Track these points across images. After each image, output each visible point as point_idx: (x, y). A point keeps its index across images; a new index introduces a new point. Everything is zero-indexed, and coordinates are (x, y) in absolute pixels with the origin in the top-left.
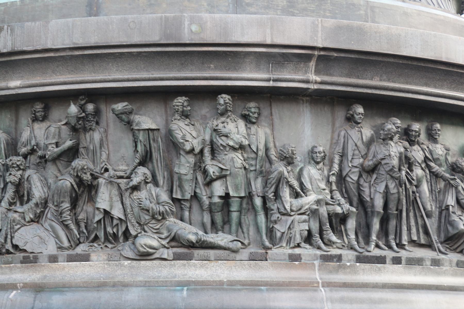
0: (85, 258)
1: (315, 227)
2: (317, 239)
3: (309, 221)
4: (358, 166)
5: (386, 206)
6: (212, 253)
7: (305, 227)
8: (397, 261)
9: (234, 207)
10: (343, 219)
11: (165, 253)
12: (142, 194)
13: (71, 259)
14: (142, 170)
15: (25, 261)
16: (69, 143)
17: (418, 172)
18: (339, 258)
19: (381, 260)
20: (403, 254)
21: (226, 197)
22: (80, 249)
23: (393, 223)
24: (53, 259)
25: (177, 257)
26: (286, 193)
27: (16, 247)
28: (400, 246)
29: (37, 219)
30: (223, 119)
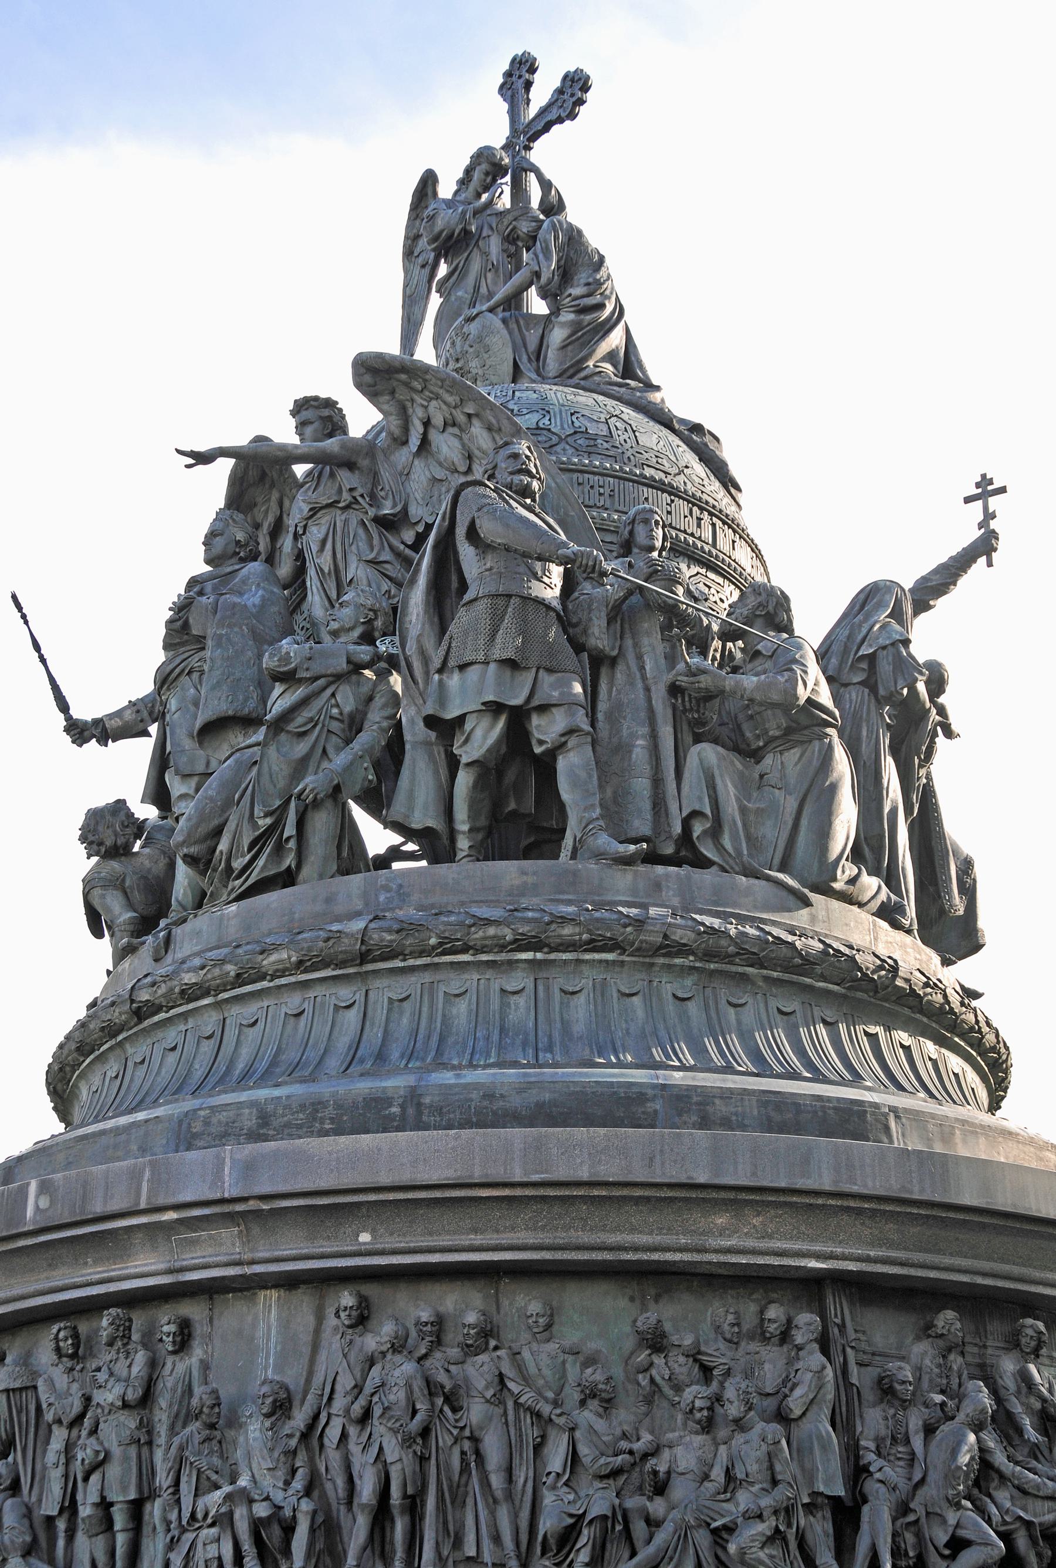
3: (218, 1540)
4: (341, 1413)
7: (212, 1551)
9: (120, 1520)
10: (289, 1529)
17: (476, 1412)
21: (105, 1505)
30: (113, 1355)
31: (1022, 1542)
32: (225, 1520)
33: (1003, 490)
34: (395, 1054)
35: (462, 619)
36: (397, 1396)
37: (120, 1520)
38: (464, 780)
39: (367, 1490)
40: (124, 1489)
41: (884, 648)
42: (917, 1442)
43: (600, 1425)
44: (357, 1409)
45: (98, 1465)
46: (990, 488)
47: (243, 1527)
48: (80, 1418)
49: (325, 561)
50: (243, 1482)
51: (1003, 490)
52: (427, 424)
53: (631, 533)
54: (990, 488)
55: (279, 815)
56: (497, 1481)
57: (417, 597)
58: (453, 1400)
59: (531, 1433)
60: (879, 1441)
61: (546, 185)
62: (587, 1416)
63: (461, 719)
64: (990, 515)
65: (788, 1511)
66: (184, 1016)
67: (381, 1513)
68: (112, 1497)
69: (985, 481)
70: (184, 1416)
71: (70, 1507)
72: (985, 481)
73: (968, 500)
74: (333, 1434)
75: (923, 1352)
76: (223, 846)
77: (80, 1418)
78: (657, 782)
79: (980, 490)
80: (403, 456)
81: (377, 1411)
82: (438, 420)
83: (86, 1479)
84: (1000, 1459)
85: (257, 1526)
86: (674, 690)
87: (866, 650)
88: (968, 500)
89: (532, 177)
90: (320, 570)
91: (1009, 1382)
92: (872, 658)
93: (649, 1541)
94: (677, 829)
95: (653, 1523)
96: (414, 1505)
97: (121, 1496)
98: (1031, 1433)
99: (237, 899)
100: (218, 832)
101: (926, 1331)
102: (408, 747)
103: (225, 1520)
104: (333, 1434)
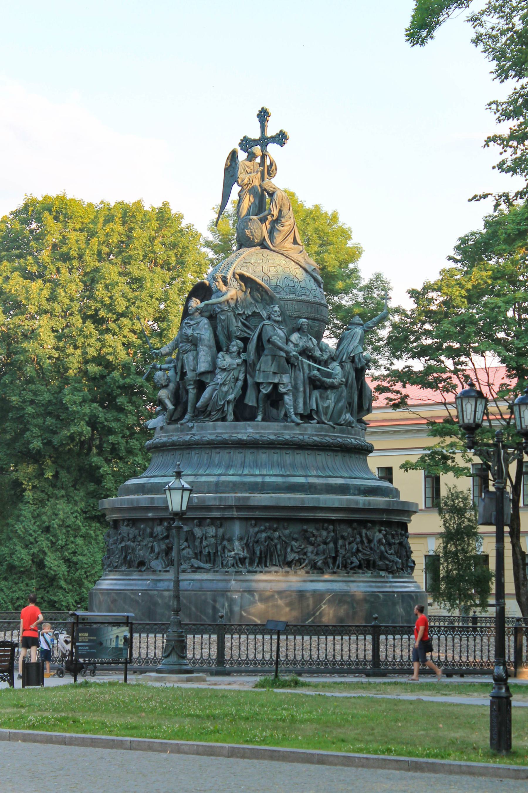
0: (168, 571)
2: (235, 565)
5: (261, 554)
8: (261, 572)
11: (189, 570)
12: (184, 552)
14: (186, 543)
15: (153, 571)
16: (165, 534)
18: (241, 572)
19: (255, 572)
20: (267, 569)
21: (209, 552)
22: (168, 569)
23: (264, 559)
24: (160, 571)
25: (193, 572)
26: (226, 551)
28: (266, 566)
29: (157, 558)
31: (362, 562)
32: (234, 558)
35: (263, 358)
38: (261, 394)
39: (258, 553)
43: (296, 544)
48: (202, 538)
50: (236, 551)
55: (224, 405)
56: (279, 553)
58: (272, 540)
59: (285, 545)
60: (341, 546)
62: (293, 543)
65: (326, 558)
67: (260, 558)
71: (201, 552)
74: (251, 545)
75: (350, 530)
76: (209, 409)
77: (202, 538)
78: (305, 398)
83: (205, 548)
84: (360, 549)
86: (310, 378)
87: (352, 355)
90: (222, 326)
91: (364, 535)
95: (304, 560)
96: (266, 557)
98: (366, 544)
100: (207, 406)
101: (351, 526)
104: (251, 545)
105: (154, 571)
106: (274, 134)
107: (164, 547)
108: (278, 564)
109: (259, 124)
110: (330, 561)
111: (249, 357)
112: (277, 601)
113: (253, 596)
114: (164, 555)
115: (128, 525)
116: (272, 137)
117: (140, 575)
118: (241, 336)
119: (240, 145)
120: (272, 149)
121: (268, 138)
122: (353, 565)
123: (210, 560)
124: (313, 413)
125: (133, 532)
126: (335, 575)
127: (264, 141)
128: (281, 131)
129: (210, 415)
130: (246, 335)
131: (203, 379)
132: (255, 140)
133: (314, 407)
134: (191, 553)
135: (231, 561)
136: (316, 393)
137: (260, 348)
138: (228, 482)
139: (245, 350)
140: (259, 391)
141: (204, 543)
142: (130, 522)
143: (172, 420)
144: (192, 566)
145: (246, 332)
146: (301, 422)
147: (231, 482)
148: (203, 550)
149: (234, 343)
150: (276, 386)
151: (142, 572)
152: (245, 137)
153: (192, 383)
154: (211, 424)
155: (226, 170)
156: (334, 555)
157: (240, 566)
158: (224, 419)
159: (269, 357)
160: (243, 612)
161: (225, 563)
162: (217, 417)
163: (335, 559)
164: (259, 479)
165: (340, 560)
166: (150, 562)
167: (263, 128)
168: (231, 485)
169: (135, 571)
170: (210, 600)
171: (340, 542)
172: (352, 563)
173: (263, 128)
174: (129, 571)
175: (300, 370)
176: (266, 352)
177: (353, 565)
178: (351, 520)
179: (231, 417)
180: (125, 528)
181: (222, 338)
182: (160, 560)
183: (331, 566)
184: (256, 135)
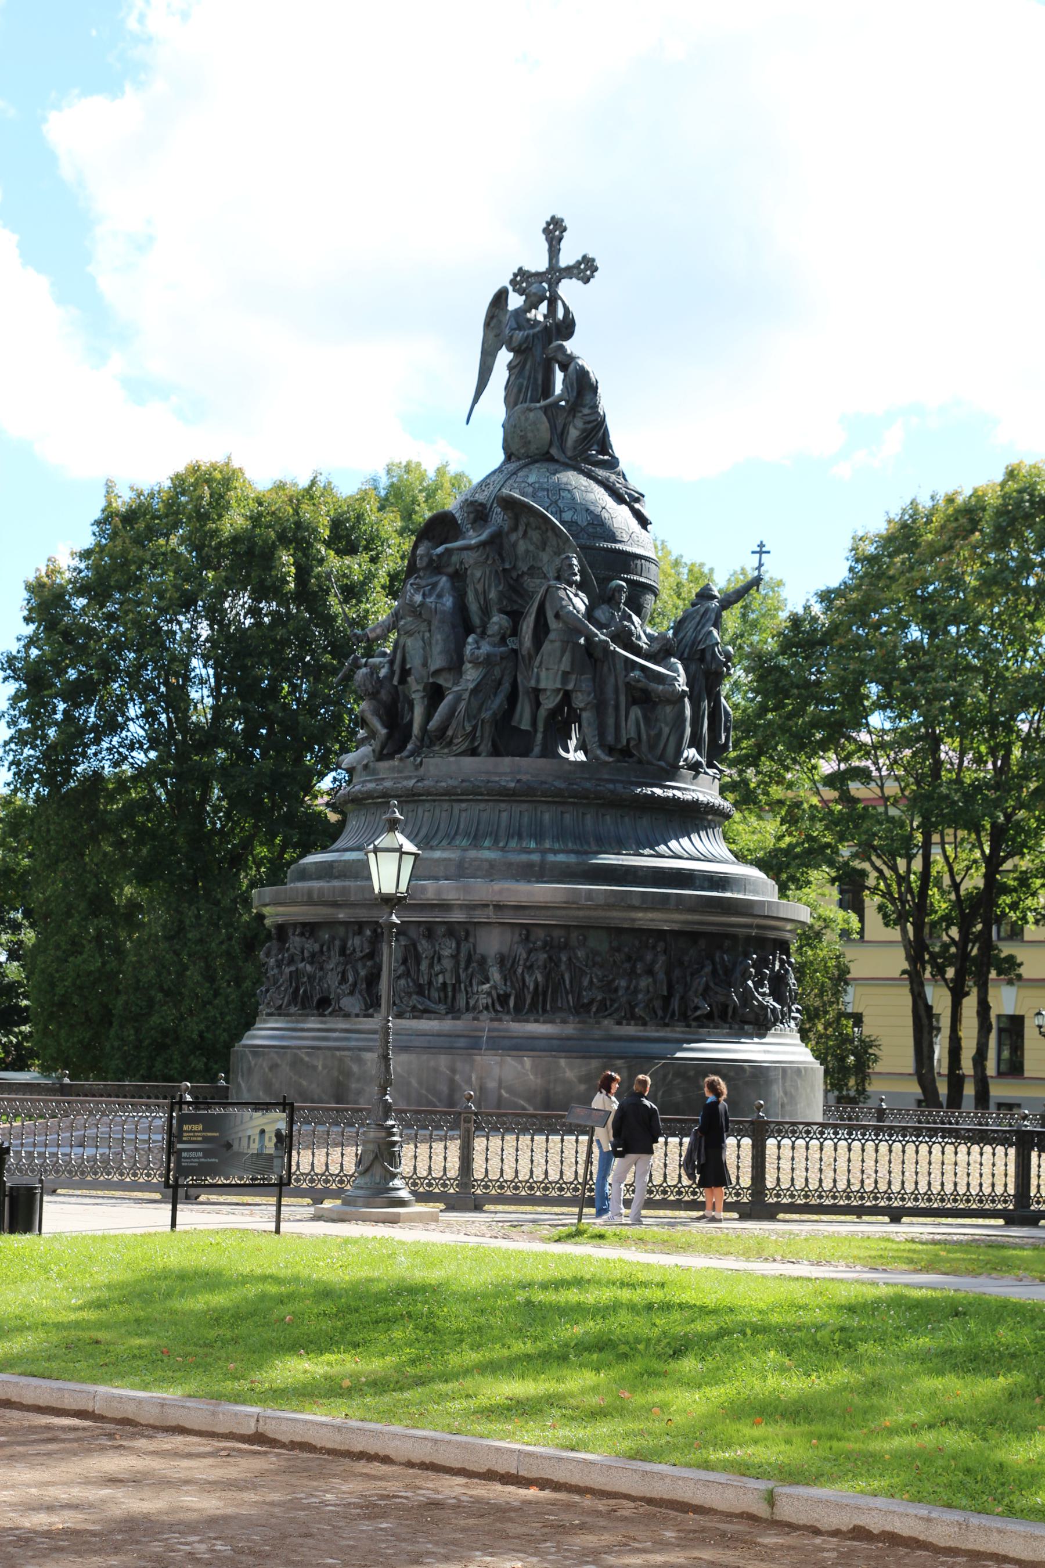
1: (490, 1001)
6: (433, 1015)
7: (485, 1001)
9: (450, 989)
10: (507, 996)
13: (366, 1016)
14: (402, 968)
17: (563, 967)
21: (444, 984)
22: (371, 1011)
24: (357, 1016)
25: (414, 1018)
27: (340, 1008)
28: (544, 1011)
32: (489, 994)
33: (768, 552)
34: (525, 834)
35: (547, 647)
36: (540, 963)
37: (450, 989)
40: (451, 979)
41: (708, 646)
42: (688, 979)
44: (528, 964)
45: (442, 972)
46: (764, 549)
47: (495, 996)
48: (433, 958)
49: (480, 587)
51: (768, 552)
52: (527, 525)
53: (613, 595)
54: (764, 549)
57: (528, 626)
58: (557, 965)
61: (567, 310)
63: (545, 690)
64: (761, 565)
66: (434, 801)
68: (448, 982)
69: (761, 545)
70: (469, 960)
71: (430, 983)
72: (761, 545)
73: (753, 552)
74: (520, 970)
76: (450, 733)
77: (433, 958)
79: (758, 549)
80: (513, 537)
81: (535, 967)
82: (534, 526)
83: (437, 975)
84: (712, 985)
85: (499, 996)
86: (628, 685)
88: (753, 552)
89: (560, 303)
91: (717, 959)
92: (703, 650)
93: (611, 1006)
94: (624, 742)
96: (545, 993)
97: (451, 980)
99: (455, 755)
102: (521, 694)
103: (489, 994)
104: (520, 970)
105: (347, 1015)
106: (572, 263)
107: (363, 973)
108: (565, 1007)
109: (546, 246)
110: (657, 1004)
111: (521, 644)
112: (565, 1072)
113: (522, 1064)
114: (364, 986)
115: (302, 934)
116: (569, 269)
117: (322, 1022)
118: (509, 609)
119: (513, 282)
120: (568, 289)
121: (561, 270)
122: (698, 1013)
123: (446, 997)
124: (632, 743)
125: (311, 946)
126: (668, 1029)
127: (555, 274)
128: (584, 257)
129: (450, 743)
130: (515, 607)
131: (441, 681)
132: (537, 274)
133: (633, 734)
134: (411, 984)
135: (484, 1000)
136: (636, 712)
137: (541, 630)
138: (482, 860)
139: (515, 632)
140: (538, 704)
141: (437, 968)
142: (308, 928)
143: (381, 756)
144: (414, 1007)
145: (516, 602)
146: (611, 759)
147: (486, 860)
148: (433, 979)
149: (495, 619)
150: (567, 696)
151: (325, 1016)
152: (520, 269)
153: (420, 687)
154: (452, 759)
155: (487, 325)
156: (665, 993)
157: (499, 1008)
158: (474, 752)
159: (558, 644)
160: (503, 1092)
161: (472, 1002)
162: (463, 748)
163: (667, 1000)
164: (535, 857)
165: (675, 1004)
166: (339, 1000)
167: (554, 251)
168: (486, 866)
169: (313, 1015)
170: (443, 1069)
171: (677, 973)
172: (697, 1008)
173: (554, 251)
174: (301, 1015)
175: (610, 669)
176: (552, 636)
177: (698, 1013)
178: (697, 932)
179: (485, 746)
180: (297, 939)
181: (473, 607)
182: (357, 995)
183: (660, 1013)
184: (539, 263)
